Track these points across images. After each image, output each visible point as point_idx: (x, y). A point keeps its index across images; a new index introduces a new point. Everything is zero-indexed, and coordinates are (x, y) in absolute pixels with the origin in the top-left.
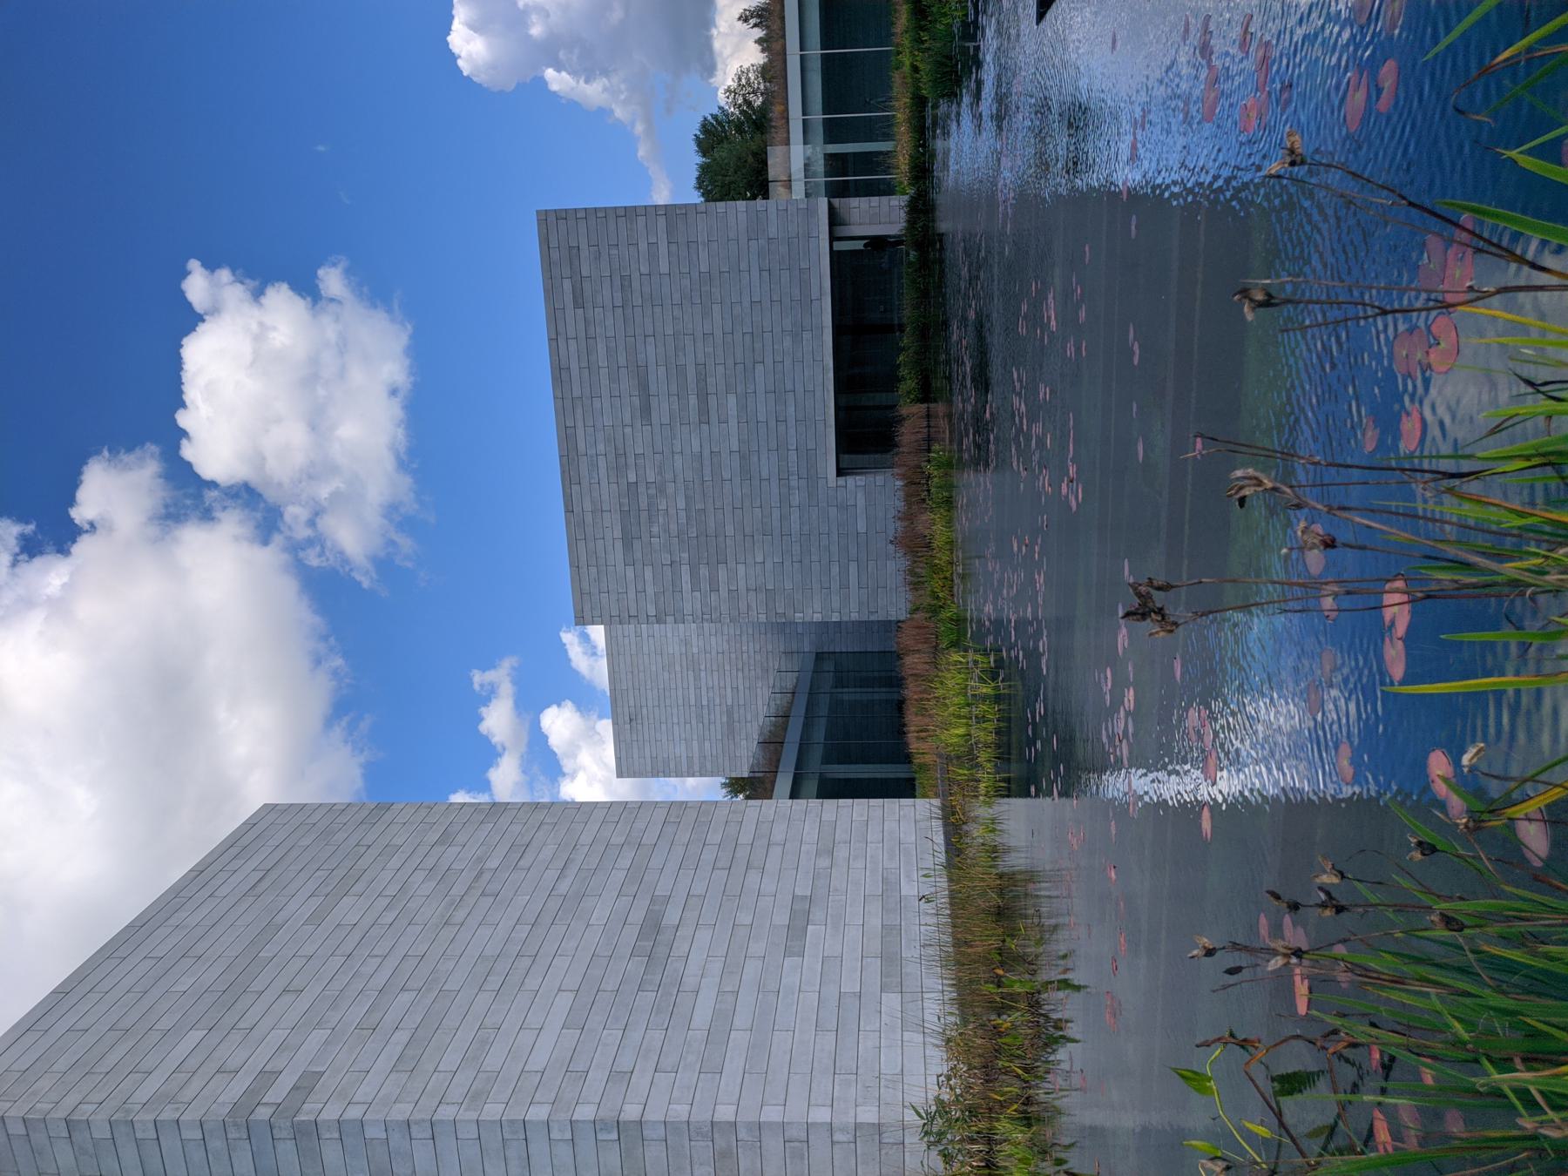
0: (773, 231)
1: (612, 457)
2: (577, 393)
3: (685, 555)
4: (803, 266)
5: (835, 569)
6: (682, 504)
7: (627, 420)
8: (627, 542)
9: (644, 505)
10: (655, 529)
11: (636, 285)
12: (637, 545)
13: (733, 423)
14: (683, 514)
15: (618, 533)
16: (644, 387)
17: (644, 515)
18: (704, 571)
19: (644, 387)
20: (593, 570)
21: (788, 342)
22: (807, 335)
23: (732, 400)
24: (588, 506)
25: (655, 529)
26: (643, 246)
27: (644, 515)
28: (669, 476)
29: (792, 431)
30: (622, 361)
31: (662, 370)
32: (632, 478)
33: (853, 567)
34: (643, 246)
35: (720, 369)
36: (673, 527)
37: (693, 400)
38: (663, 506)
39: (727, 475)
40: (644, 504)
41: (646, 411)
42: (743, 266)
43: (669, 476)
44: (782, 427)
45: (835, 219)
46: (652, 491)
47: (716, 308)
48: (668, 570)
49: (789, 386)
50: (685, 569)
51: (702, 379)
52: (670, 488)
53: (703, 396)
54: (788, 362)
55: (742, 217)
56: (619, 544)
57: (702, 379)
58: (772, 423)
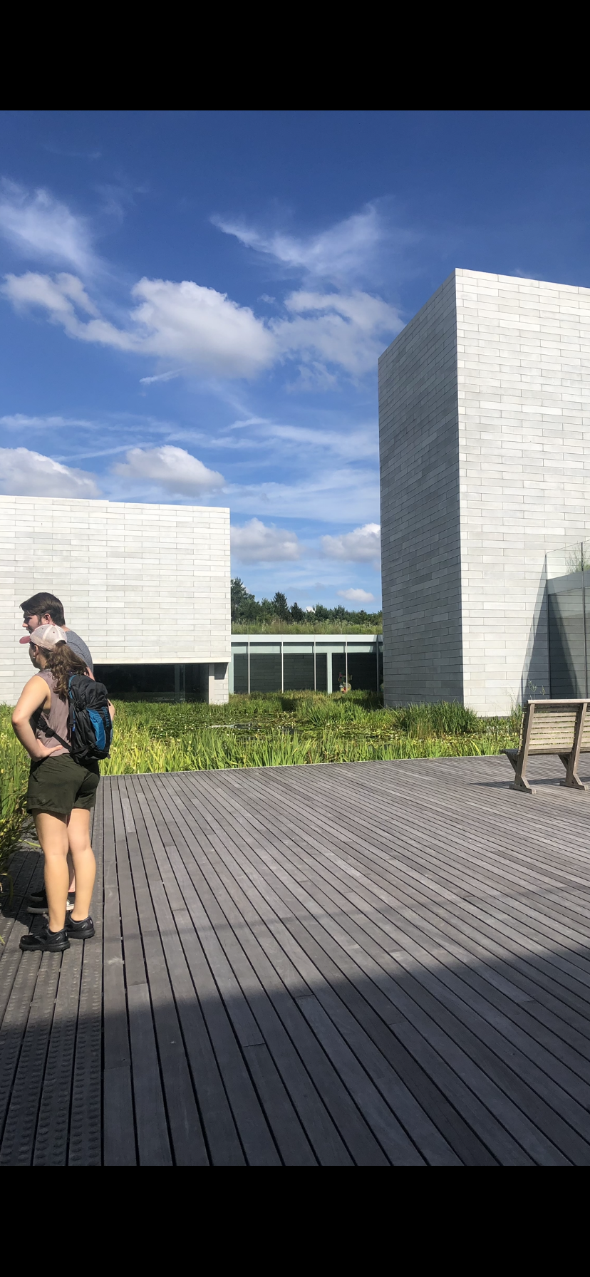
0: (213, 633)
1: (88, 532)
2: (127, 517)
3: (21, 569)
4: (196, 648)
5: (8, 662)
6: (56, 570)
7: (110, 543)
8: (31, 535)
9: (56, 547)
10: (39, 553)
11: (188, 557)
12: (30, 540)
13: (106, 605)
14: (49, 570)
15: (37, 530)
16: (131, 555)
17: (50, 547)
18: (11, 580)
19: (131, 555)
20: (13, 512)
21: (153, 638)
22: (157, 648)
23: (122, 605)
24: (55, 514)
25: (39, 553)
26: (209, 563)
27: (50, 547)
28: (74, 564)
29: (100, 639)
30: (145, 545)
31: (140, 567)
32: (73, 542)
33: (10, 673)
34: (209, 563)
35: (139, 600)
36: (41, 564)
37: (122, 583)
38: (55, 558)
39: (74, 599)
40: (56, 547)
41: (116, 555)
42: (197, 616)
43: (74, 564)
44: (104, 633)
45: (219, 669)
46: (65, 553)
47: (174, 600)
48: (12, 558)
49: (127, 638)
50: (12, 569)
51: (134, 589)
52: (68, 565)
53: (124, 588)
54: (143, 638)
55: (223, 617)
56: (31, 530)
57: (134, 589)
58: (105, 628)
